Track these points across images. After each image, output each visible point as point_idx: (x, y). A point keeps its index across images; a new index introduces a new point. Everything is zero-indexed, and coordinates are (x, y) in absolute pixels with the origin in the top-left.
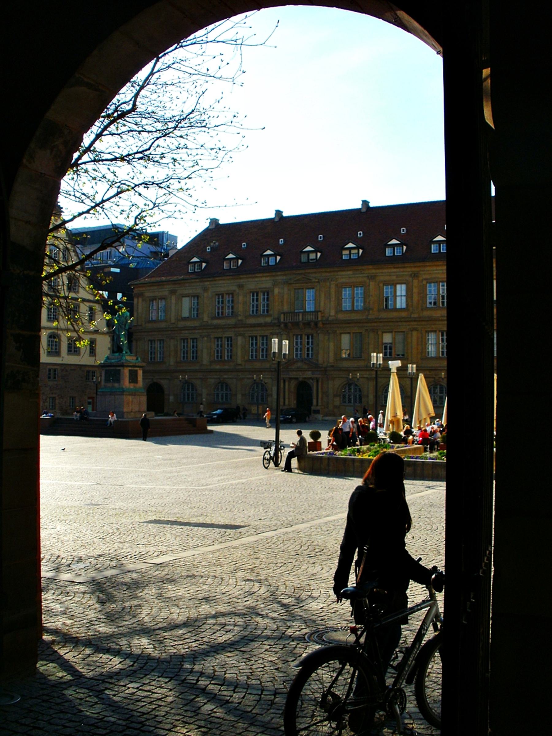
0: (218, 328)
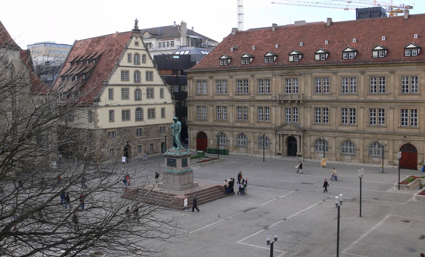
0: (239, 101)
